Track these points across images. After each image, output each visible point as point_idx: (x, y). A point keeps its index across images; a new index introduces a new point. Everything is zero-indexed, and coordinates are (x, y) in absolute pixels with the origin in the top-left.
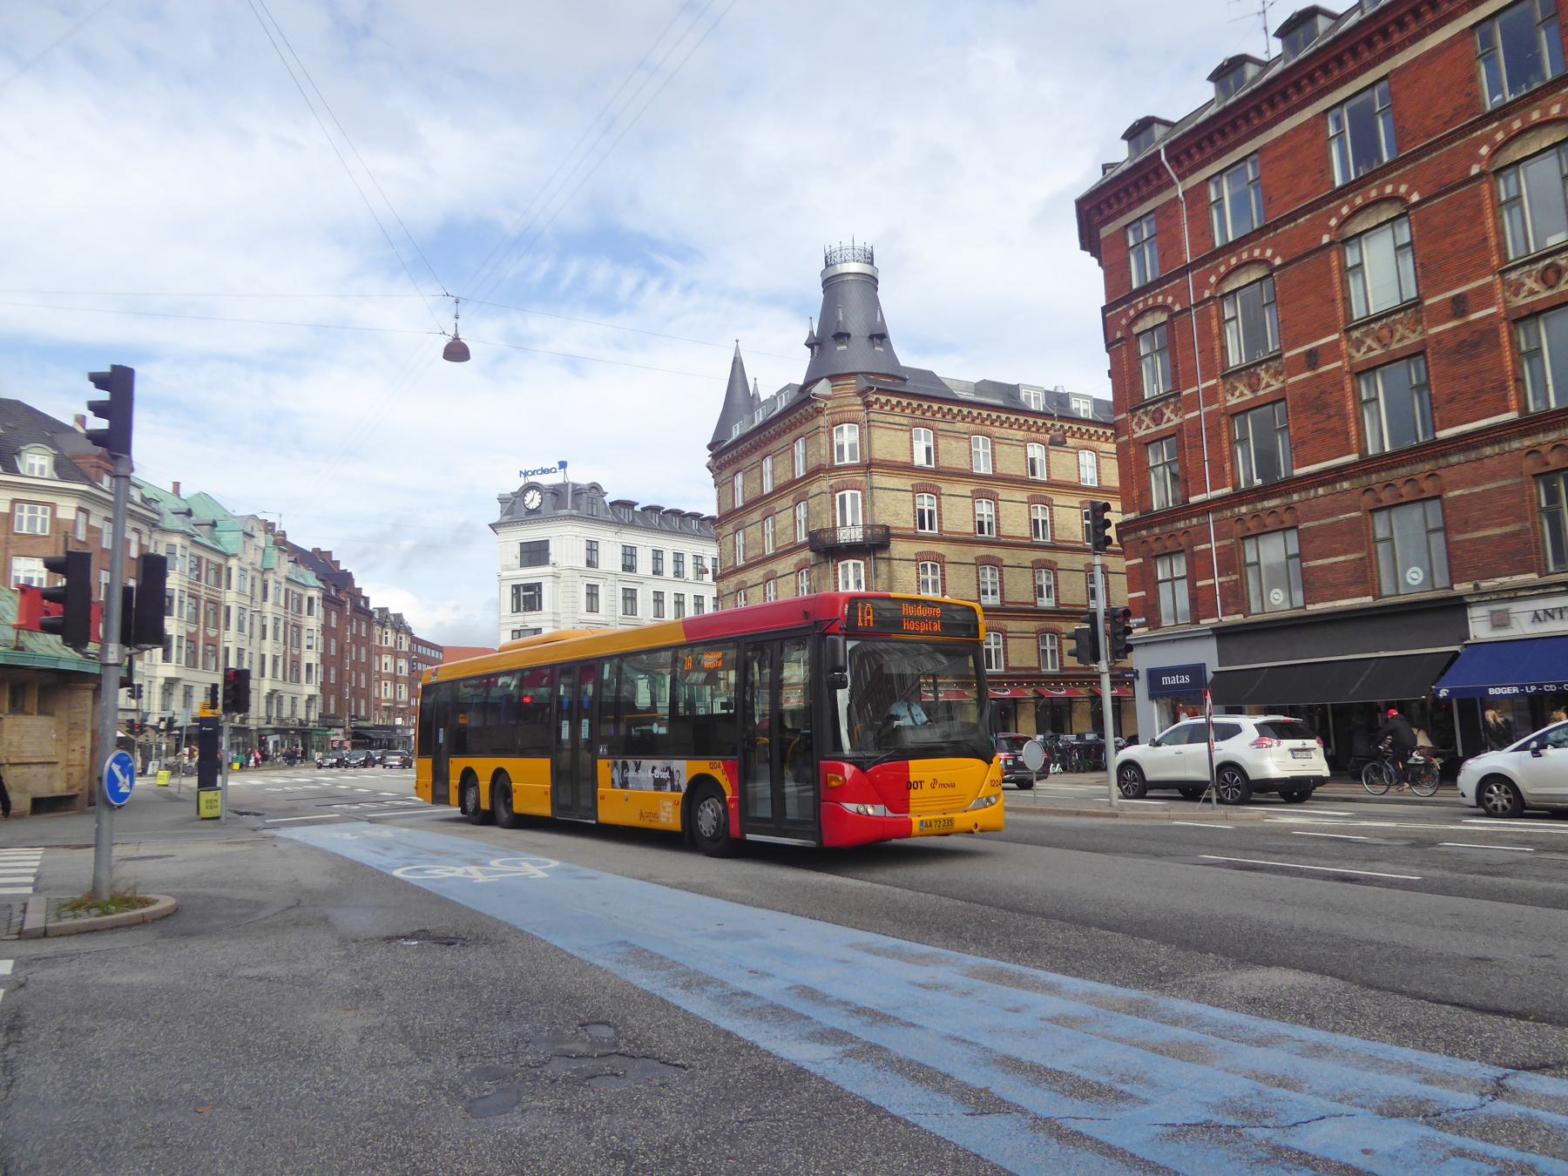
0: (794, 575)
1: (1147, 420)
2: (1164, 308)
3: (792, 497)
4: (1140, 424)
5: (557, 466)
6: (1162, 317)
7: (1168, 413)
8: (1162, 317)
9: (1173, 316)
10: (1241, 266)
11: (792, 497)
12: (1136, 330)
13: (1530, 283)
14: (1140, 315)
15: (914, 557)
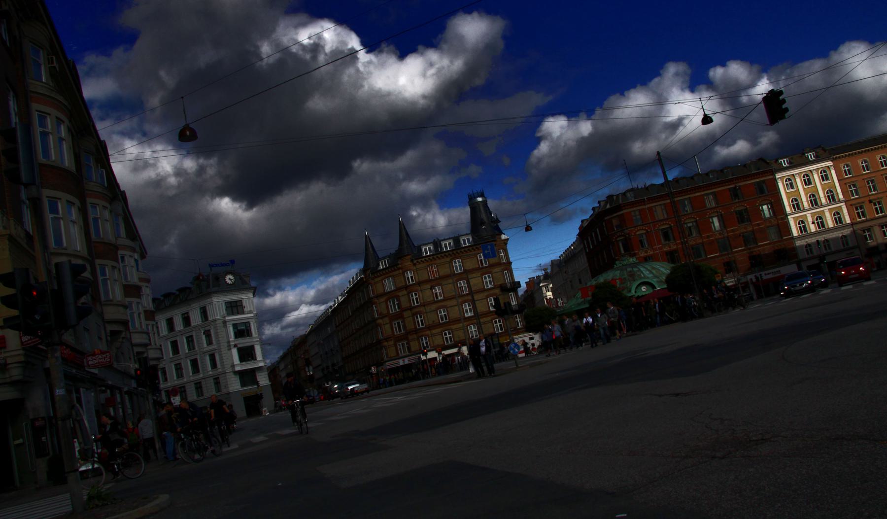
0: (486, 300)
1: (643, 253)
2: (645, 230)
3: (480, 273)
4: (641, 253)
5: (229, 262)
6: (645, 232)
7: (649, 251)
8: (645, 232)
9: (648, 232)
10: (664, 224)
11: (480, 273)
12: (637, 233)
13: (718, 235)
14: (638, 230)
15: (485, 297)
